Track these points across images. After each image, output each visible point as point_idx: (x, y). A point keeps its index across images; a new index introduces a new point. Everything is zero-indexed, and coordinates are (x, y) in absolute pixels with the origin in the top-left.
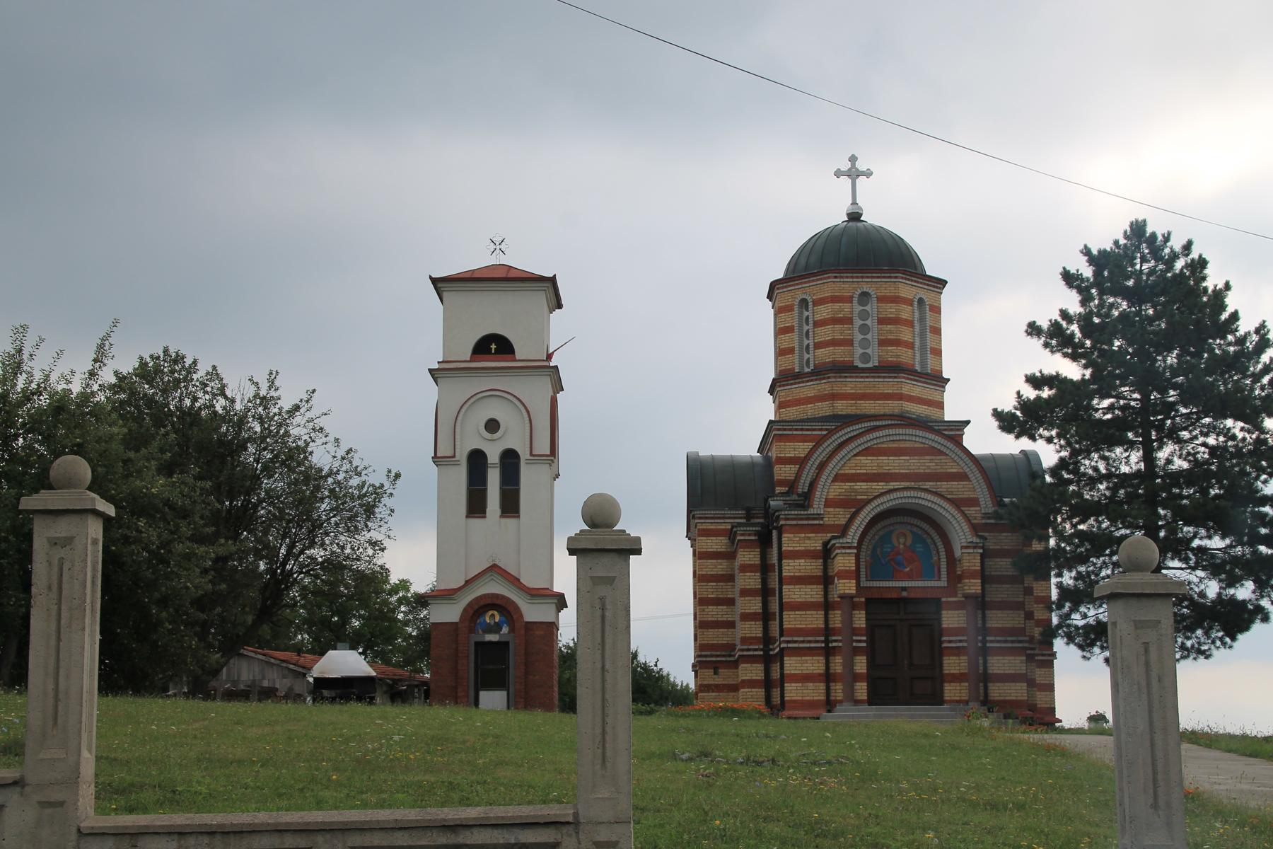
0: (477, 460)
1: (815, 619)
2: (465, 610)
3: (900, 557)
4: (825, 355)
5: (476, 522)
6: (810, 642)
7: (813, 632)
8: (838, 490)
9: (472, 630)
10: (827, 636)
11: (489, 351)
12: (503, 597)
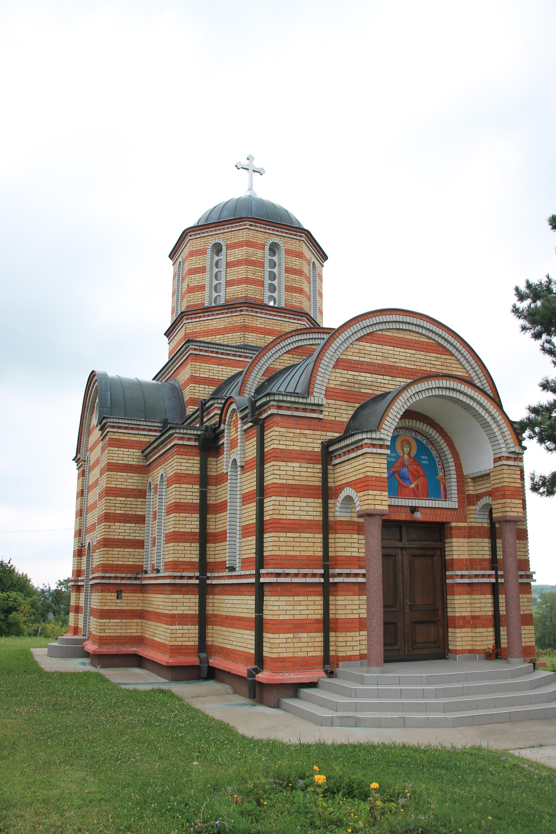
1: (310, 545)
3: (405, 470)
4: (238, 292)
6: (305, 575)
7: (308, 562)
8: (339, 378)
10: (326, 568)
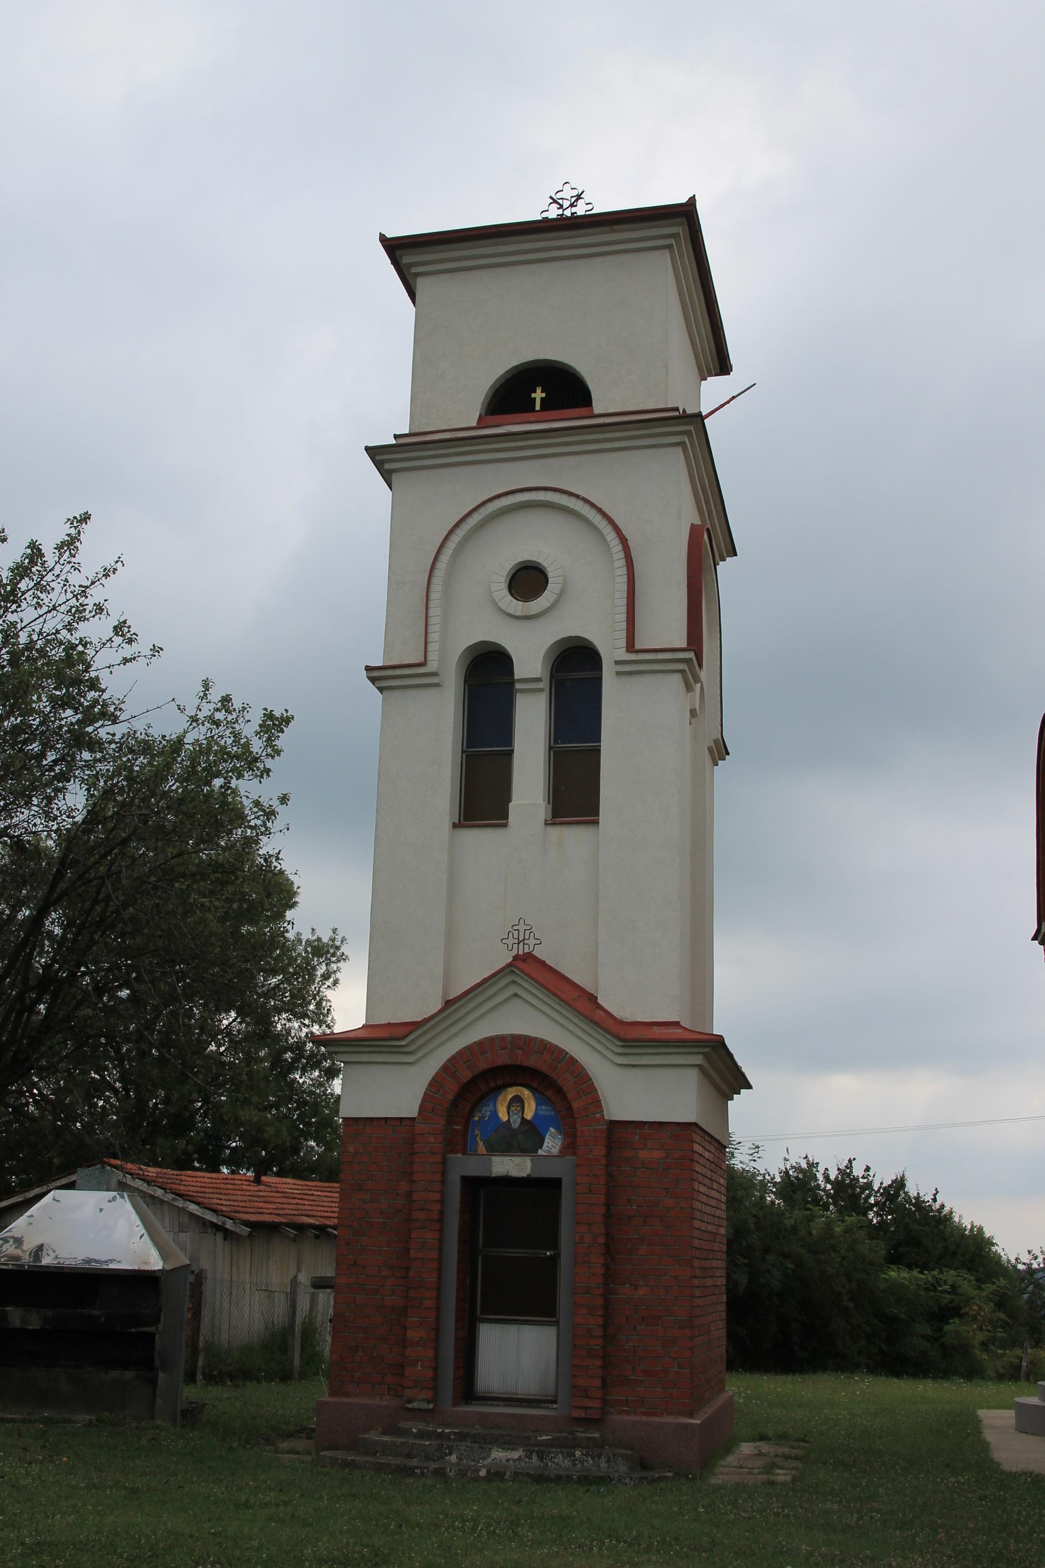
0: (488, 672)
2: (435, 1084)
5: (480, 840)
9: (458, 1141)
11: (529, 406)
12: (544, 1046)
